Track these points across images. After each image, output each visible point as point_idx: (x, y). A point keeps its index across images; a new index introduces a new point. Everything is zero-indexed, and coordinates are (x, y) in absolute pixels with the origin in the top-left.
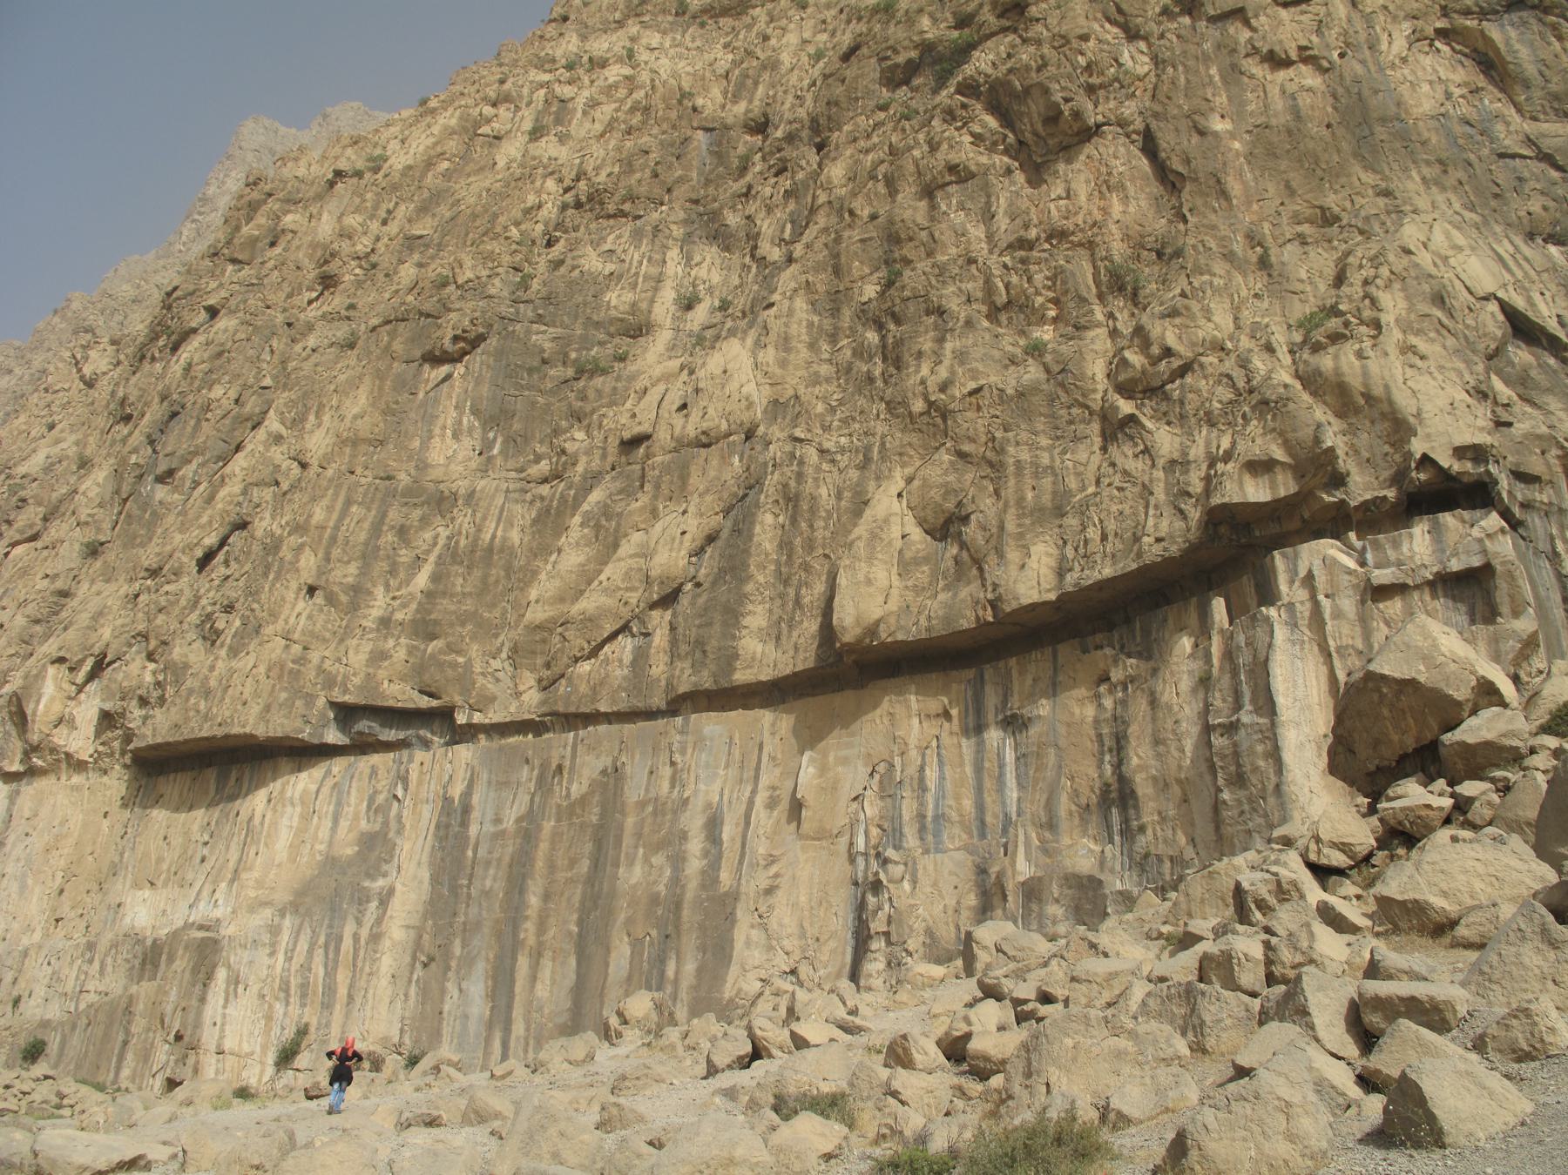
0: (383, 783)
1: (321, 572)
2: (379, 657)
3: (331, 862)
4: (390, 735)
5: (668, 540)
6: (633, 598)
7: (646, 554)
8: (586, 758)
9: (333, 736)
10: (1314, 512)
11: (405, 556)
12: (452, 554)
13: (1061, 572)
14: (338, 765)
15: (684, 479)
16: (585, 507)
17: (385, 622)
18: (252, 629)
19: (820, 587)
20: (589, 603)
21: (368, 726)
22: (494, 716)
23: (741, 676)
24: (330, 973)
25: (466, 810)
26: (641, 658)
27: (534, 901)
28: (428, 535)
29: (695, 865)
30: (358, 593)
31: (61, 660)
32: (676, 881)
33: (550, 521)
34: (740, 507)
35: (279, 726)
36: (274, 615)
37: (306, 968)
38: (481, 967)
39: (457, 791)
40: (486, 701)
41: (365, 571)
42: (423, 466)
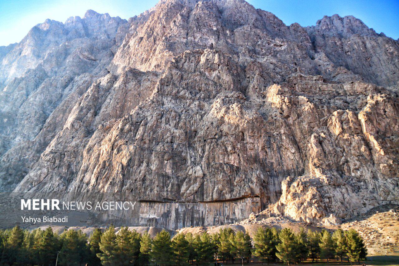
0: (169, 206)
1: (159, 184)
2: (167, 194)
3: (165, 213)
6: (193, 192)
7: (193, 188)
13: (231, 196)
15: (196, 180)
17: (167, 191)
19: (211, 194)
25: (178, 209)
27: (186, 217)
28: (169, 181)
29: (201, 216)
30: (163, 187)
34: (202, 185)
35: (159, 200)
36: (154, 188)
38: (182, 222)
39: (177, 207)
40: (178, 200)
41: (163, 185)
42: (166, 173)
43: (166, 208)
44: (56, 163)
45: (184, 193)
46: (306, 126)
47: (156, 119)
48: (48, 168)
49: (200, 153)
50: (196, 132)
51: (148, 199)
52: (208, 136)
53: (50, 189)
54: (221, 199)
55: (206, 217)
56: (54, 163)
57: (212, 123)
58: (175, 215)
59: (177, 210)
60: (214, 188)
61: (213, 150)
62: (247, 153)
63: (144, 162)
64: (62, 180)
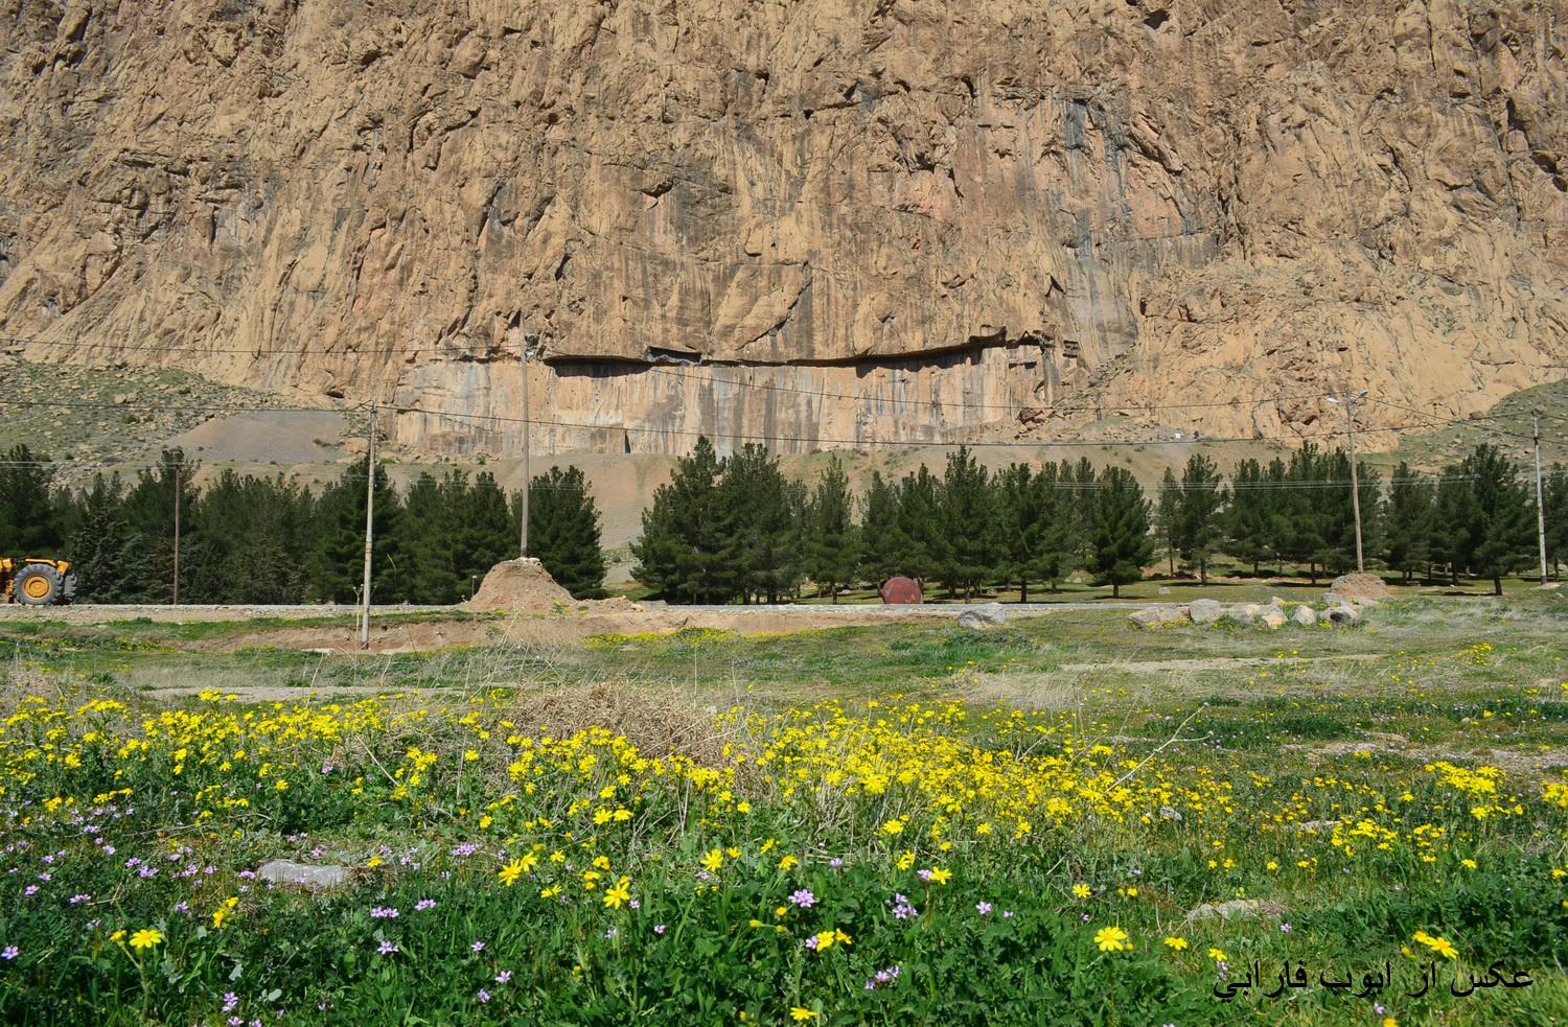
3: (657, 405)
4: (673, 360)
5: (778, 302)
8: (762, 376)
9: (650, 359)
10: (999, 340)
11: (660, 288)
12: (685, 293)
13: (925, 342)
14: (651, 372)
15: (780, 276)
16: (736, 279)
17: (663, 317)
18: (600, 314)
19: (841, 332)
20: (750, 321)
21: (662, 356)
22: (716, 357)
23: (817, 357)
24: (665, 443)
25: (711, 390)
26: (774, 344)
27: (745, 422)
29: (803, 415)
30: (647, 303)
31: (498, 313)
32: (797, 418)
33: (723, 280)
34: (804, 290)
36: (611, 306)
37: (656, 440)
43: (662, 385)
44: (151, 208)
45: (732, 327)
46: (1239, 60)
47: (594, 15)
48: (117, 231)
49: (787, 164)
50: (766, 77)
51: (588, 352)
52: (819, 94)
53: (141, 320)
54: (883, 349)
55: (823, 421)
56: (143, 207)
57: (836, 41)
58: (698, 411)
59: (706, 395)
60: (855, 306)
61: (847, 152)
62: (985, 169)
63: (558, 198)
64: (193, 280)
